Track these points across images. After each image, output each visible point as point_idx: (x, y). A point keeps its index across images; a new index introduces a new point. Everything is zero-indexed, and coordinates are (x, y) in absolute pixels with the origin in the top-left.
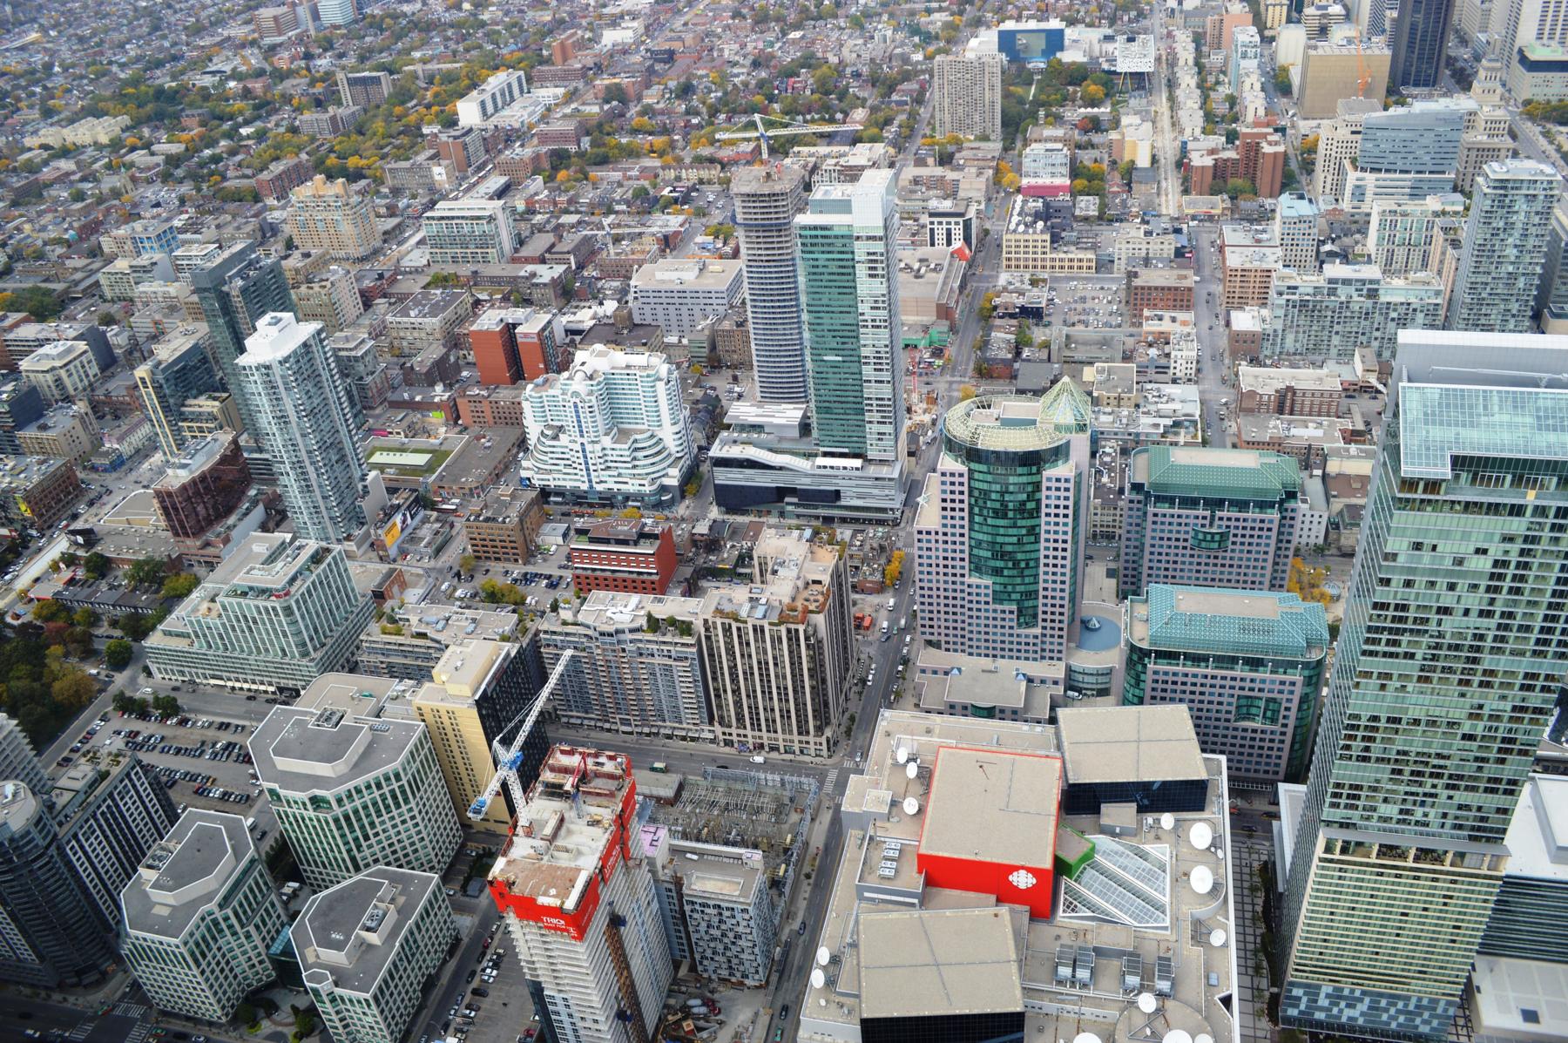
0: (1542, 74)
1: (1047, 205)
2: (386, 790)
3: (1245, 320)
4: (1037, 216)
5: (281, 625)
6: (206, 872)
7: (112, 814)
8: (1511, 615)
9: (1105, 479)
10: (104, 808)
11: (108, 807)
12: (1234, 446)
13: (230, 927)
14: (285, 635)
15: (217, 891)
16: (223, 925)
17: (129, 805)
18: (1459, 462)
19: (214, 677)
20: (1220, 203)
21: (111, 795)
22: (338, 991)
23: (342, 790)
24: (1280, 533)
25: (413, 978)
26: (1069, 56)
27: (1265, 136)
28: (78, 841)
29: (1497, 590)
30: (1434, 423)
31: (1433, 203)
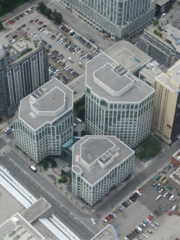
2: (130, 110)
5: (115, 9)
6: (53, 109)
7: (27, 65)
10: (25, 62)
11: (27, 62)
13: (53, 132)
14: (115, 13)
15: (54, 117)
16: (51, 131)
17: (34, 64)
19: (79, 12)
21: (29, 58)
22: (82, 177)
23: (114, 102)
25: (110, 184)
28: (12, 71)
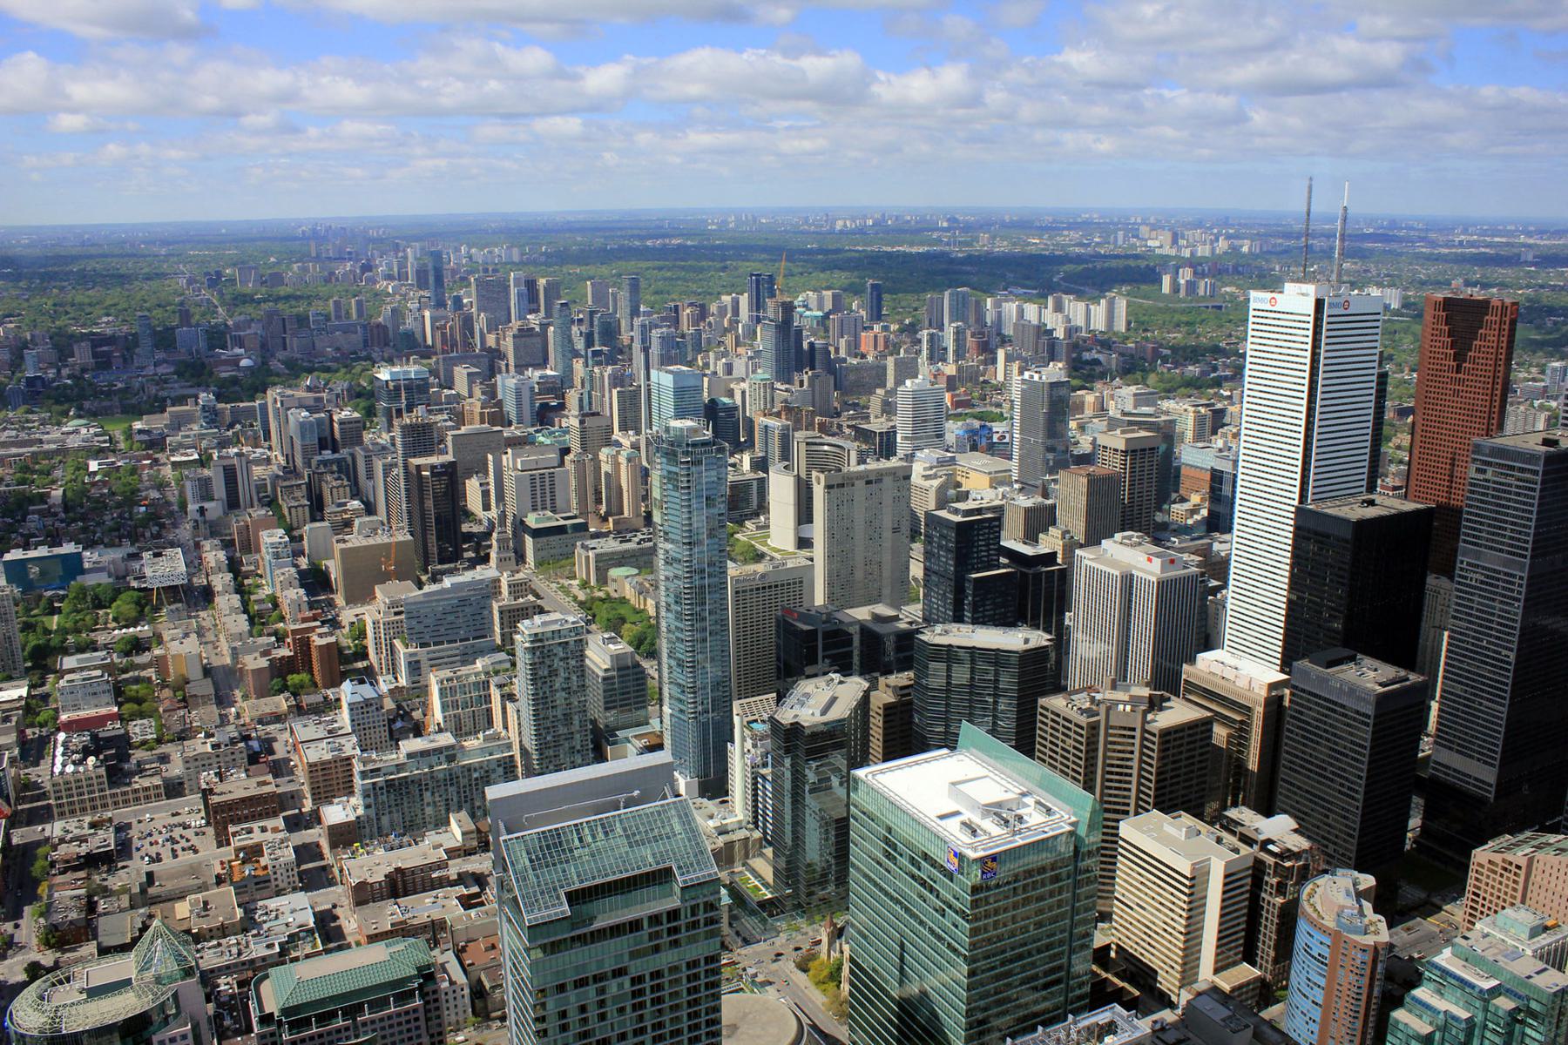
0: (544, 539)
1: (94, 737)
3: (336, 813)
4: (86, 752)
8: (660, 1025)
9: (227, 1022)
12: (358, 944)
18: (573, 898)
20: (282, 702)
24: (428, 1020)
26: (90, 580)
27: (313, 629)
29: (642, 1005)
30: (541, 867)
31: (479, 664)
